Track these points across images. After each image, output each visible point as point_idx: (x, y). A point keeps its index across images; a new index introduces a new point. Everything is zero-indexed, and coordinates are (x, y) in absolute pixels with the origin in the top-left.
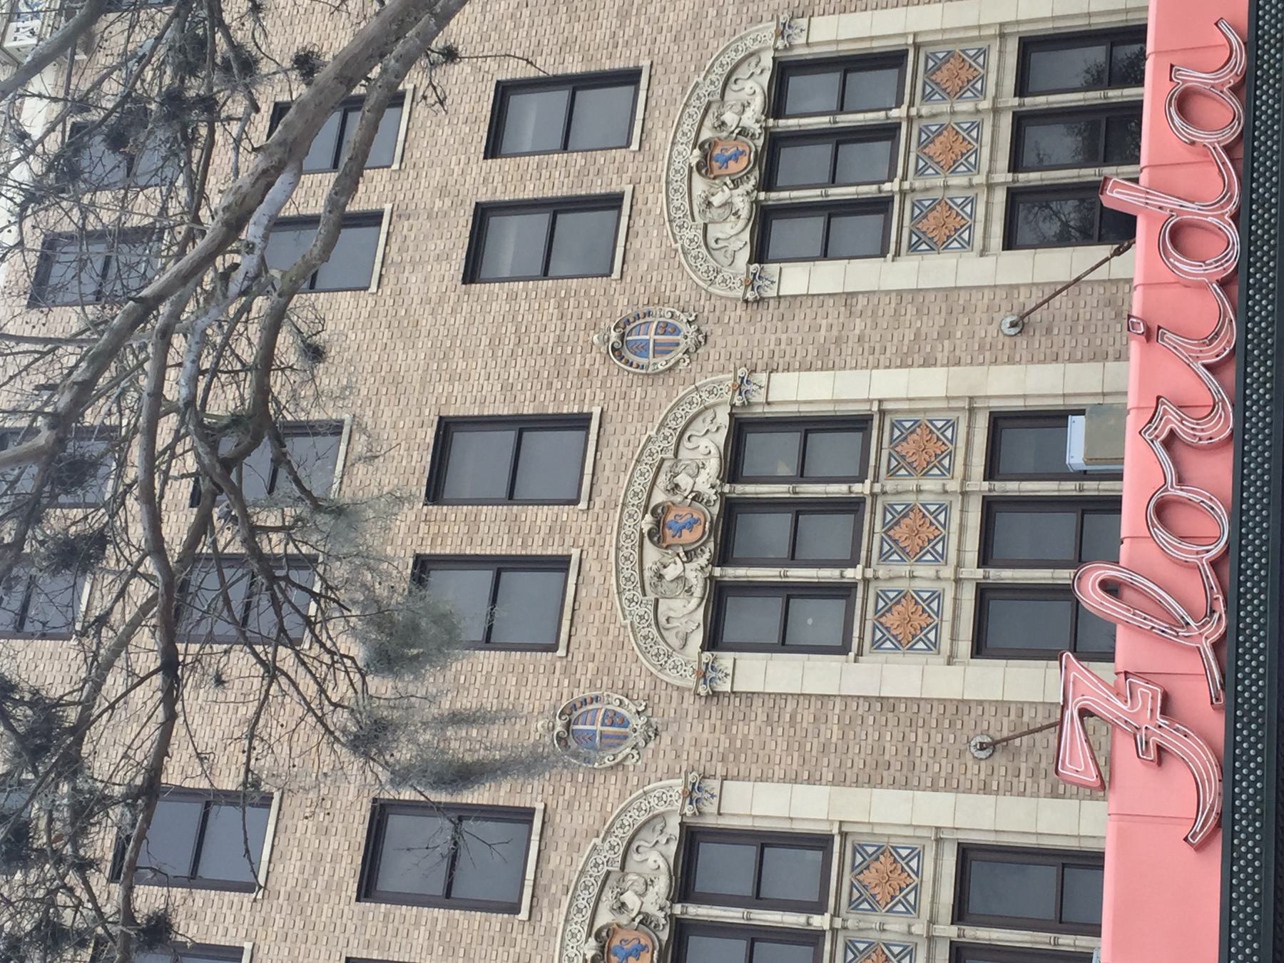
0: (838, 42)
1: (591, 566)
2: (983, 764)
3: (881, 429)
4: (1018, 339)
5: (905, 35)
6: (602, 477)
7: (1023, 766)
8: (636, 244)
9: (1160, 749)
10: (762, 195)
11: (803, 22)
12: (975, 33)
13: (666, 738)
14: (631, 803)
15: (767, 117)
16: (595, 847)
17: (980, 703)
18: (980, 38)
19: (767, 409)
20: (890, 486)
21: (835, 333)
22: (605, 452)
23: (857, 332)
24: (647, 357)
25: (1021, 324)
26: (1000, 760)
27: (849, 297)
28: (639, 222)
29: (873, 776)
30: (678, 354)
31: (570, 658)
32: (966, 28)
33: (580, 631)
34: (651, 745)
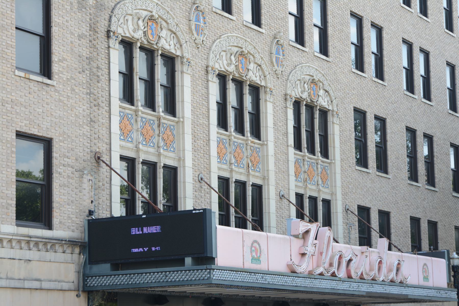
0: (333, 134)
1: (232, 24)
2: (197, 178)
3: (259, 144)
4: (279, 197)
5: (334, 160)
6: (250, 30)
7: (197, 193)
8: (296, 50)
9: (303, 255)
10: (305, 103)
11: (338, 123)
12: (334, 185)
13: (197, 51)
14: (183, 35)
15: (320, 106)
16: (174, 19)
17: (210, 177)
18: (332, 186)
19: (264, 100)
20: (249, 147)
21: (280, 128)
22: (254, 33)
23: (280, 137)
24: (277, 54)
25: (282, 197)
26: (198, 185)
27: (287, 133)
28: (300, 52)
29: (195, 138)
30: (276, 67)
31: (212, 13)
32: (335, 181)
33: (218, 17)
34: (194, 44)
